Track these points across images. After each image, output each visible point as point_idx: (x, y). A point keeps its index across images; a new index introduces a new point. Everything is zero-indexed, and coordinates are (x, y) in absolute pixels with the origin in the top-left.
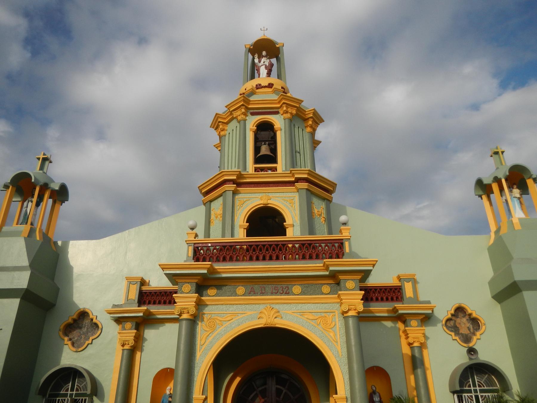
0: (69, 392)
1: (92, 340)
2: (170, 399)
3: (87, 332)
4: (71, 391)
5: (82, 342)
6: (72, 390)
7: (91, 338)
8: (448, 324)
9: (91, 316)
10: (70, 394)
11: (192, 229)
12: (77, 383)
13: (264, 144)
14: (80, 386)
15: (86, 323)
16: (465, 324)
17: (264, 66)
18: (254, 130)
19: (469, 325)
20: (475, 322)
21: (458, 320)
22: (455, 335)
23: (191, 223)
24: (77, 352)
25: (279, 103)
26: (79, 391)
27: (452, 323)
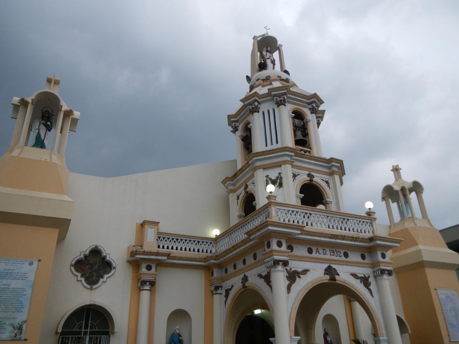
0: (83, 330)
1: (107, 278)
2: (180, 338)
4: (84, 329)
5: (94, 279)
6: (86, 327)
7: (106, 276)
9: (104, 254)
10: (84, 331)
12: (91, 321)
13: (299, 130)
14: (94, 323)
15: (96, 261)
17: (270, 60)
18: (293, 116)
24: (91, 289)
25: (309, 99)
26: (93, 329)
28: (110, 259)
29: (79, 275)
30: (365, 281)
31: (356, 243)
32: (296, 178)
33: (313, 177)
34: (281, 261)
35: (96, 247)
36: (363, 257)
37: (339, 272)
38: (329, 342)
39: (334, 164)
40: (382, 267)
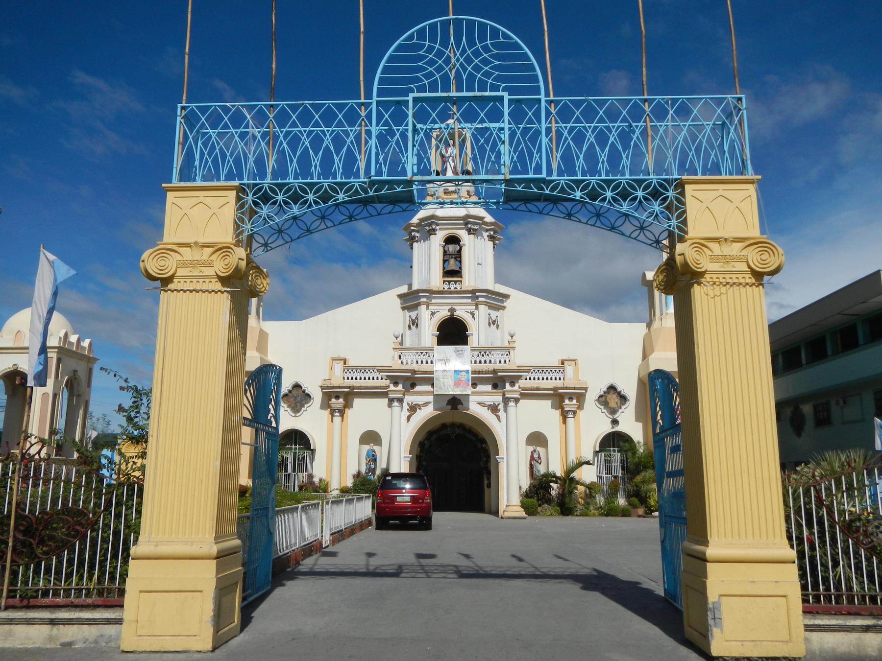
1: (307, 407)
2: (374, 453)
3: (300, 402)
7: (306, 406)
8: (600, 399)
9: (303, 388)
11: (397, 338)
12: (299, 440)
13: (452, 258)
16: (614, 399)
19: (617, 400)
20: (623, 399)
21: (609, 396)
22: (604, 408)
23: (397, 334)
27: (603, 399)
28: (308, 392)
29: (285, 406)
30: (494, 409)
31: (480, 375)
32: (434, 316)
33: (455, 310)
34: (395, 398)
35: (296, 383)
36: (495, 386)
37: (462, 402)
38: (536, 459)
39: (477, 294)
40: (507, 396)
